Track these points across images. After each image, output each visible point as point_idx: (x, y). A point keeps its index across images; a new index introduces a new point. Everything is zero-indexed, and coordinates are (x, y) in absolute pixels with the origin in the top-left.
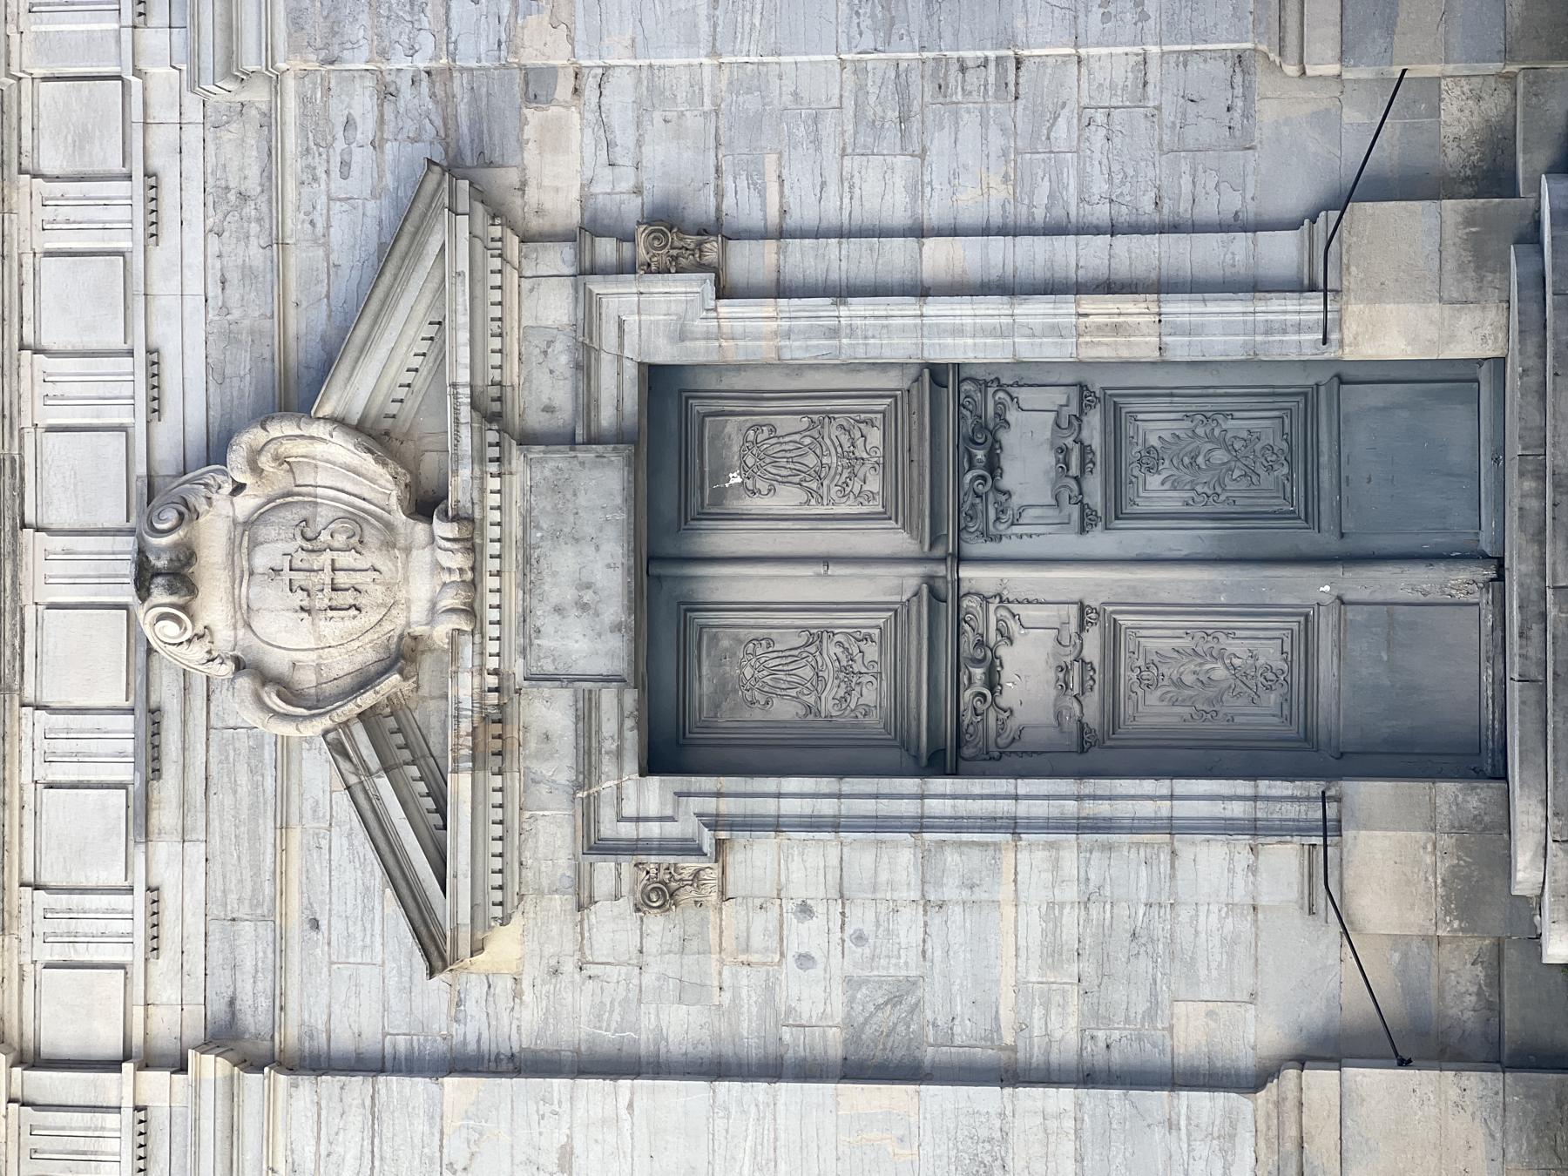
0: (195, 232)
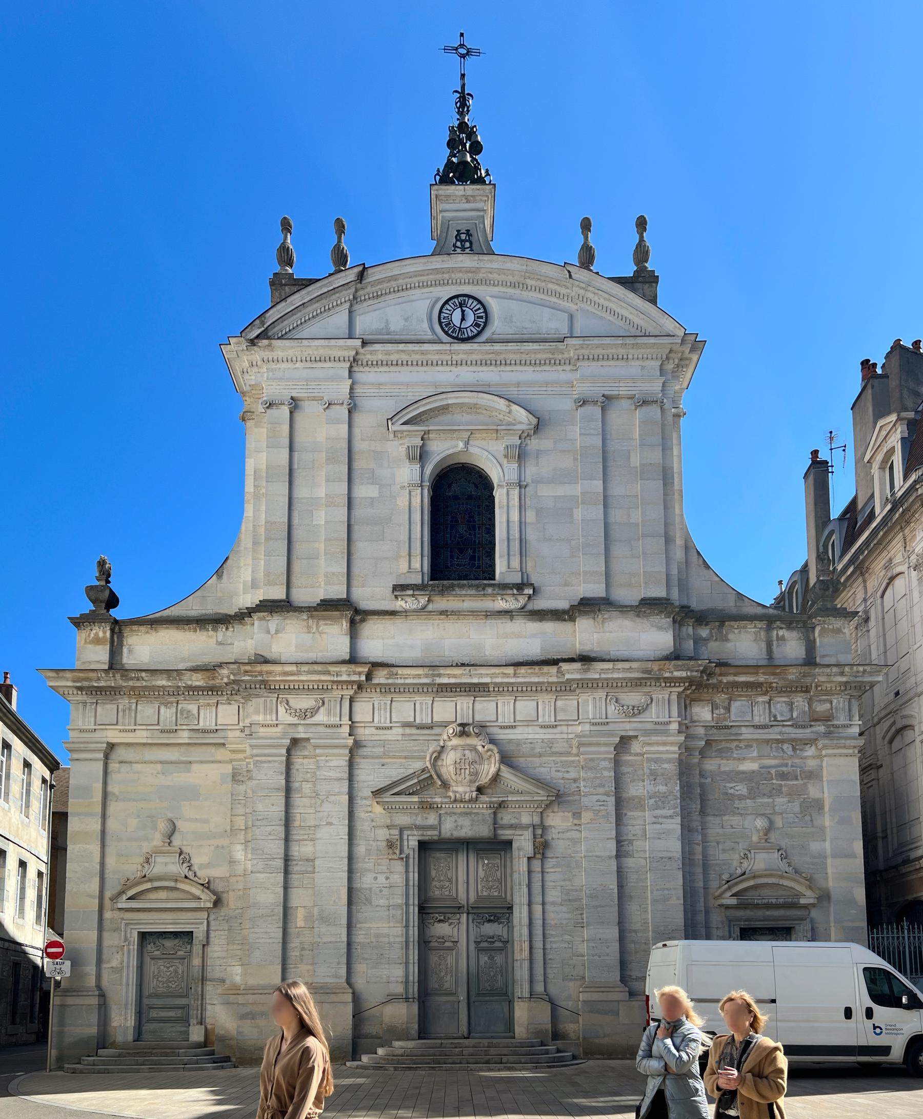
0: (542, 736)
